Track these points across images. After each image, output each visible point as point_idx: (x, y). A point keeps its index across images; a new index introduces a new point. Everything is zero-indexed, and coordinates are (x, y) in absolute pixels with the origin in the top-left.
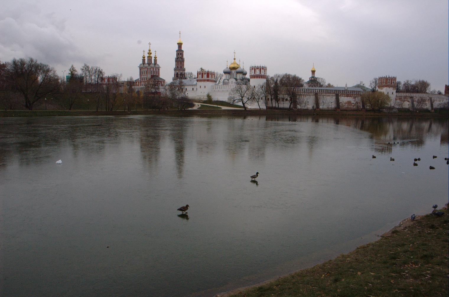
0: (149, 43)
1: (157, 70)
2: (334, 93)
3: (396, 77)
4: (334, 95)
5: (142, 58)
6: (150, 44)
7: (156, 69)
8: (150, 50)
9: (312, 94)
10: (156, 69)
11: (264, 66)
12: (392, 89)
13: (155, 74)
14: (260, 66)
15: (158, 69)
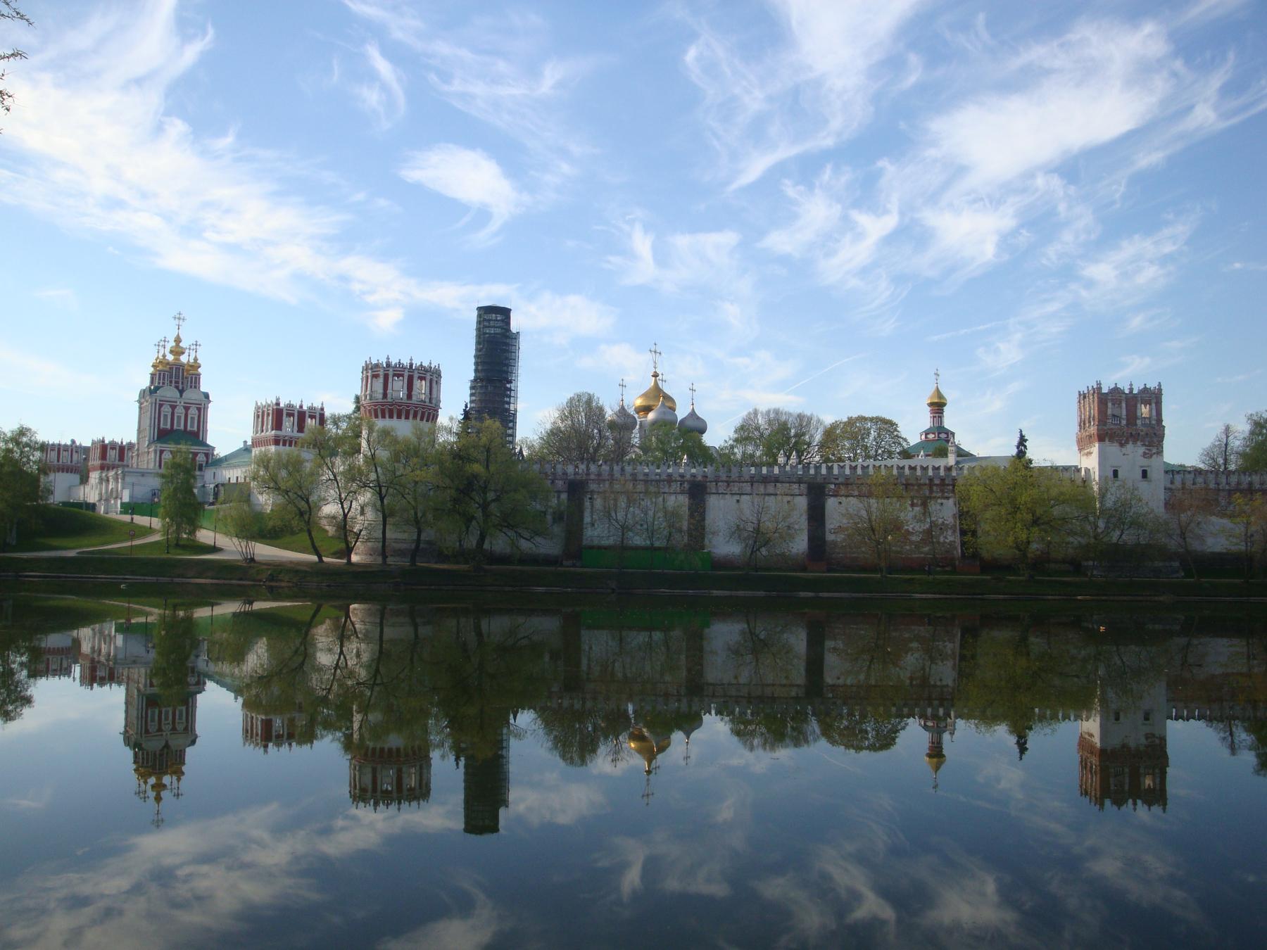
0: (175, 313)
1: (193, 412)
2: (800, 482)
3: (1160, 390)
4: (797, 492)
5: (152, 370)
6: (179, 317)
7: (187, 409)
8: (178, 340)
9: (675, 487)
10: (187, 409)
11: (426, 364)
12: (1141, 450)
13: (182, 427)
14: (411, 365)
15: (199, 409)
